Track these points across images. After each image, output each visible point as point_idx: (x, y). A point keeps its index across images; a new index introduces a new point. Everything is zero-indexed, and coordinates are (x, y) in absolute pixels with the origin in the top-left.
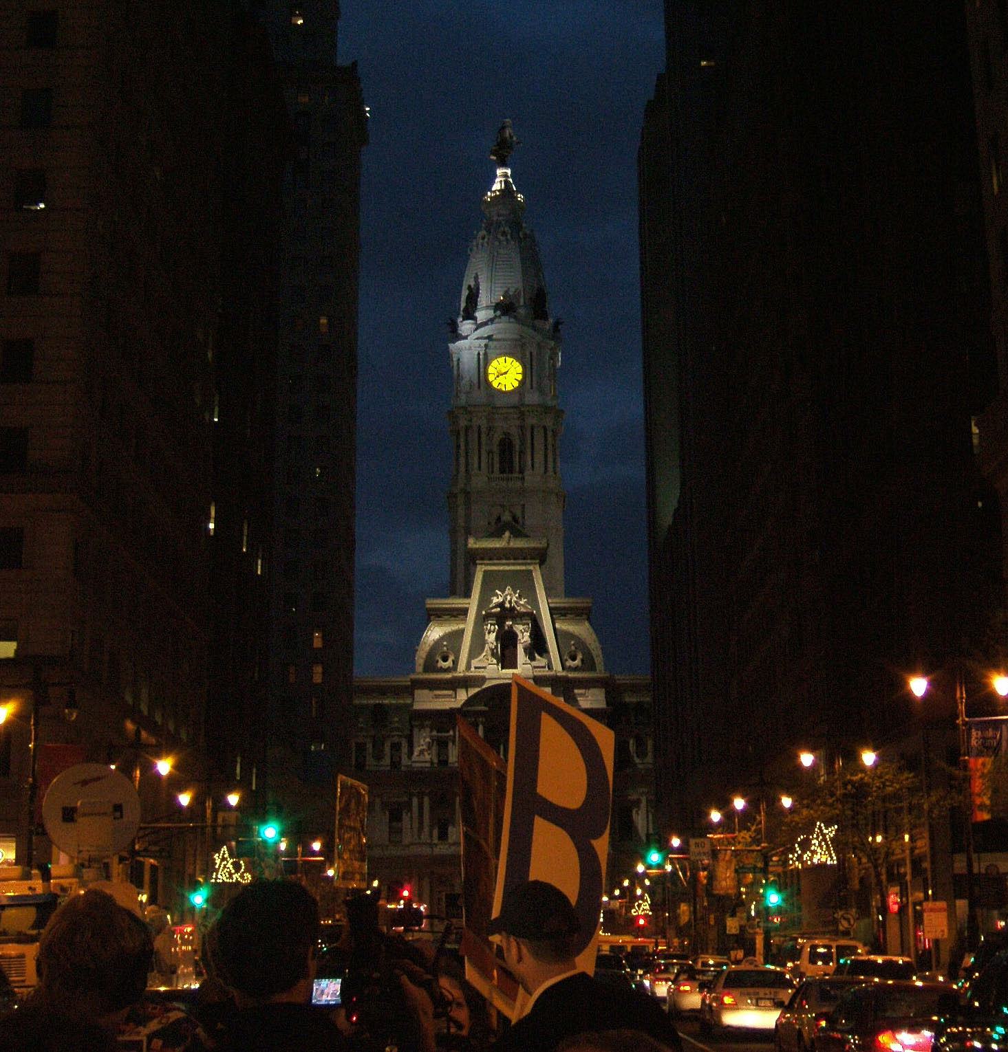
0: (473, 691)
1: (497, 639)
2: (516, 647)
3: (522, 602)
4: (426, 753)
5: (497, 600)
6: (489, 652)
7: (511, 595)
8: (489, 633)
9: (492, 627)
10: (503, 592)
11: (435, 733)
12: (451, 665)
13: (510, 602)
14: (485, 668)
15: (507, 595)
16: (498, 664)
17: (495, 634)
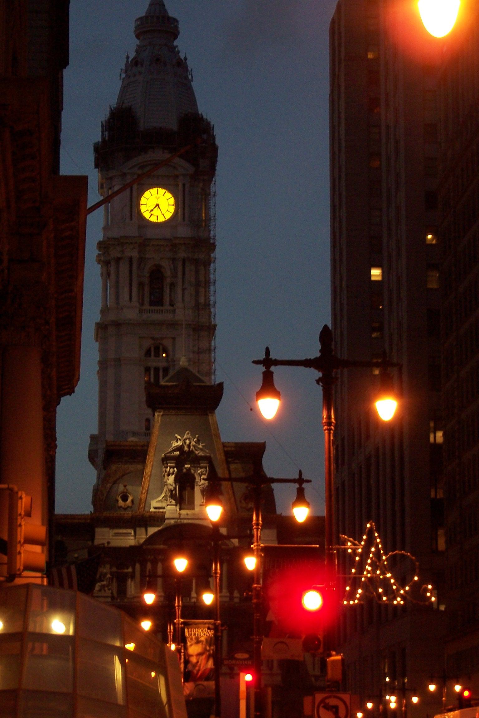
0: (152, 530)
1: (176, 481)
2: (193, 488)
3: (200, 446)
4: (106, 589)
5: (177, 444)
6: (169, 494)
7: (189, 439)
8: (169, 475)
9: (172, 470)
10: (182, 437)
11: (114, 569)
12: (130, 505)
13: (189, 446)
14: (164, 508)
15: (186, 439)
16: (176, 505)
17: (173, 476)
